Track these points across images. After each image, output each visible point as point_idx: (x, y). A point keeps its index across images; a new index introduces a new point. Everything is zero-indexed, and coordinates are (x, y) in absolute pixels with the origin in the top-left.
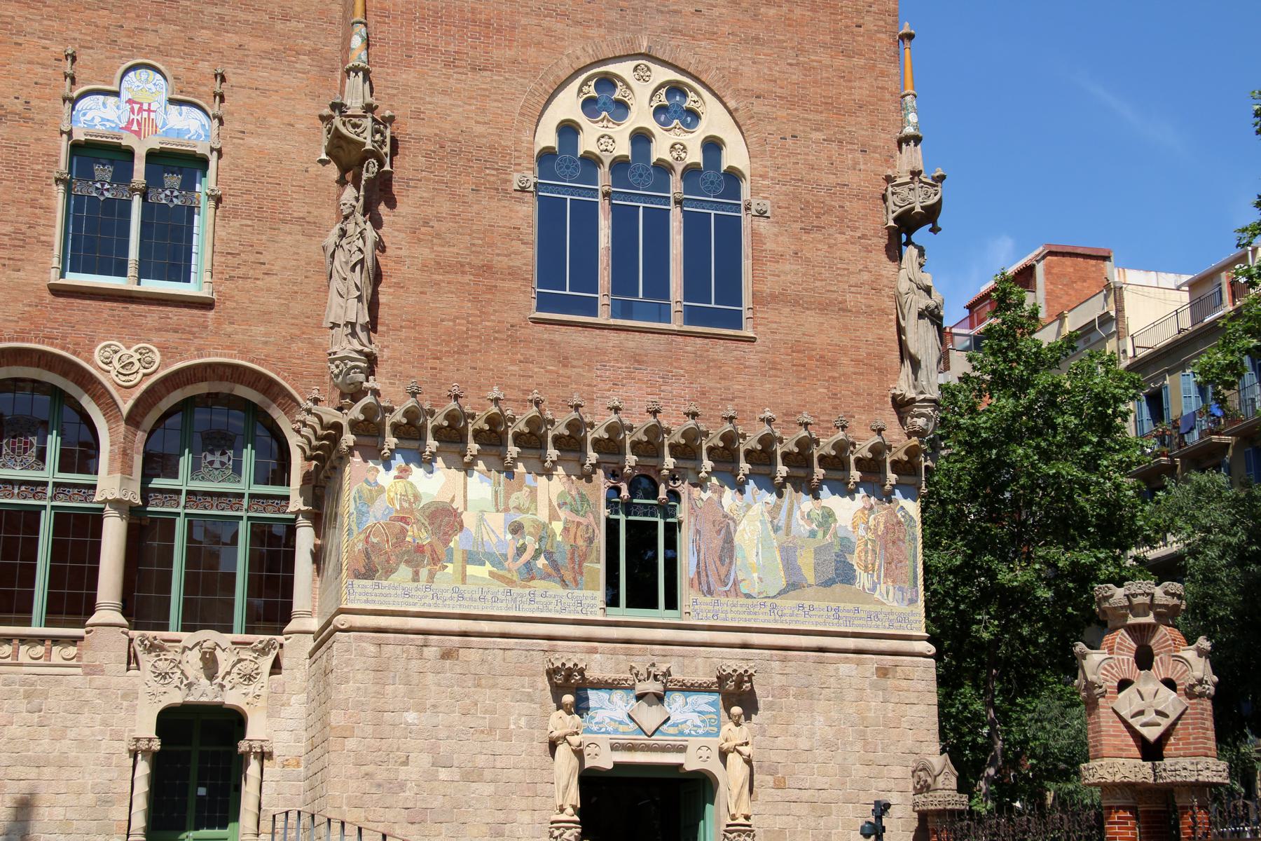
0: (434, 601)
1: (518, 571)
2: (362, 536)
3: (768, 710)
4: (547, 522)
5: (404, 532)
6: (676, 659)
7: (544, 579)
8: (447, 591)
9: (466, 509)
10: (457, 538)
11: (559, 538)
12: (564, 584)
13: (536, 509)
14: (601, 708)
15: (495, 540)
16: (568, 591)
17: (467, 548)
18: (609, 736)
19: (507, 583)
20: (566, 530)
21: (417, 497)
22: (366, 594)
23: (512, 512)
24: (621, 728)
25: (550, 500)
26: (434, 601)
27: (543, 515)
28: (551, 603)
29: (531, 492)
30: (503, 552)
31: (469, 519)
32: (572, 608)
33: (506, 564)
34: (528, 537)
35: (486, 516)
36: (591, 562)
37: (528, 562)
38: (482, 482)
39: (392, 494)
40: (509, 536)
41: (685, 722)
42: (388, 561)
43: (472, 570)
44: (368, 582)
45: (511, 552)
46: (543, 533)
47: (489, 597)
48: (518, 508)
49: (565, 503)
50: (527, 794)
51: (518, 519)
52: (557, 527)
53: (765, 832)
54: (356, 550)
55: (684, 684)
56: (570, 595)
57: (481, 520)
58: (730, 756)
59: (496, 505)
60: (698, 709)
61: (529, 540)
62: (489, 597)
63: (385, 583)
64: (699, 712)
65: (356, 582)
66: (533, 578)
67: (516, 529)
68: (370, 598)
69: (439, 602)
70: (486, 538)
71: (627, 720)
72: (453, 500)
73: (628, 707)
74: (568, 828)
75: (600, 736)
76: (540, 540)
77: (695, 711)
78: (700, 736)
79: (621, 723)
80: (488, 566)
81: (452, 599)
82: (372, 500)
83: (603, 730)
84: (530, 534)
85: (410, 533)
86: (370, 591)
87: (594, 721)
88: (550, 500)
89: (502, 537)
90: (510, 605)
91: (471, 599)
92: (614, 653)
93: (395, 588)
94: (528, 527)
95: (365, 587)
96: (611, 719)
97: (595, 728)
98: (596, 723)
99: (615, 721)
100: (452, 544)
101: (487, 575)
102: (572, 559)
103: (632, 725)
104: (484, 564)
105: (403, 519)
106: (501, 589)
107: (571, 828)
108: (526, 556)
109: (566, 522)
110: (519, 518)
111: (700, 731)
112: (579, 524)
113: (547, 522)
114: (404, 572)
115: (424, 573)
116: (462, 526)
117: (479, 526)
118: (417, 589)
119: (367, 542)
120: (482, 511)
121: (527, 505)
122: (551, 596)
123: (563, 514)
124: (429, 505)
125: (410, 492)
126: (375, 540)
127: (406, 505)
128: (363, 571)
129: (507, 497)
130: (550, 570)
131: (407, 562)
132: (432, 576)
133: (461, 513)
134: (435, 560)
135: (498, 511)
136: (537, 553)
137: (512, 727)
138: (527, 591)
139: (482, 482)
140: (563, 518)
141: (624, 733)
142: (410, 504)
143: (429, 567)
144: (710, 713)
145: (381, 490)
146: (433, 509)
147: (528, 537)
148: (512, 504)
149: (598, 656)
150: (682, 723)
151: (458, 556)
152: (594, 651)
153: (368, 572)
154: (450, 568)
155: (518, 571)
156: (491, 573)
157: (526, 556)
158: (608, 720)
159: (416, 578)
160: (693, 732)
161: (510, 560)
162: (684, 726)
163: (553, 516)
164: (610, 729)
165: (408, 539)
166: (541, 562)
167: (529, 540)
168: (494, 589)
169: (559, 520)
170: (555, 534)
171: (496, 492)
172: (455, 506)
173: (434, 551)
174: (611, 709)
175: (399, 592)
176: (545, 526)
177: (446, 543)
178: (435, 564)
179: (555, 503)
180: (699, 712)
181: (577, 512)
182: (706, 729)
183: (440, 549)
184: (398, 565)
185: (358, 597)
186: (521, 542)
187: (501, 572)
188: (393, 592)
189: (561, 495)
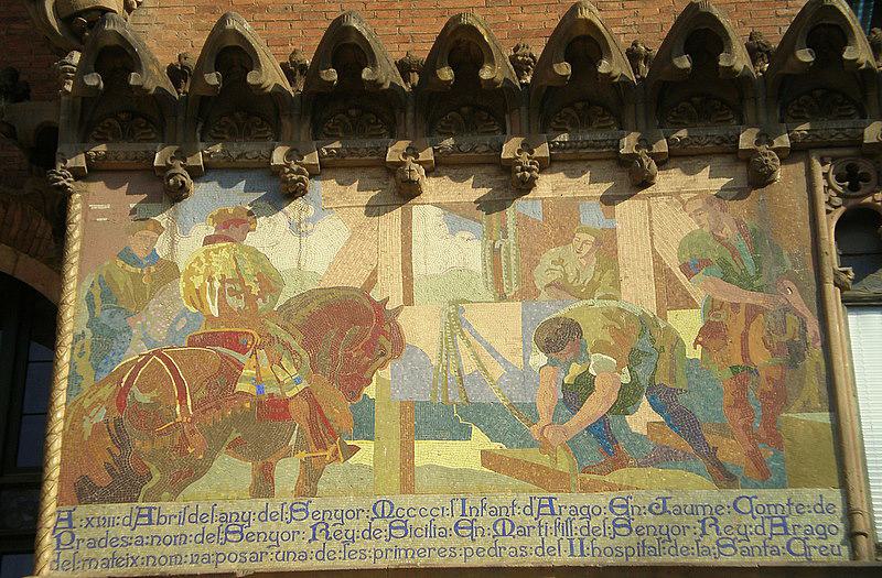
0: (317, 545)
1: (572, 446)
2: (107, 391)
4: (651, 308)
5: (231, 372)
7: (656, 462)
8: (356, 514)
9: (409, 300)
10: (385, 374)
11: (693, 353)
12: (724, 476)
13: (616, 283)
15: (497, 371)
16: (738, 492)
17: (416, 397)
19: (540, 483)
20: (711, 333)
21: (269, 282)
22: (113, 542)
23: (544, 296)
25: (657, 259)
26: (317, 545)
27: (639, 294)
28: (683, 529)
29: (598, 242)
30: (519, 399)
31: (421, 327)
32: (755, 541)
33: (534, 430)
34: (595, 358)
35: (470, 313)
36: (806, 408)
37: (603, 420)
38: (453, 232)
39: (198, 281)
40: (539, 359)
42: (181, 448)
43: (431, 453)
44: (120, 510)
45: (546, 398)
46: (637, 342)
47: (485, 521)
48: (558, 286)
49: (707, 263)
51: (562, 313)
52: (686, 324)
54: (87, 426)
56: (744, 506)
57: (456, 322)
59: (498, 283)
61: (598, 363)
62: (485, 521)
63: (170, 508)
65: (82, 511)
66: (619, 463)
67: (559, 338)
68: (121, 552)
69: (335, 545)
70: (469, 366)
72: (371, 282)
76: (634, 359)
80: (479, 439)
81: (371, 534)
82: (141, 299)
84: (601, 347)
85: (246, 372)
86: (124, 531)
88: (657, 259)
89: (518, 361)
90: (551, 542)
91: (430, 531)
93: (202, 519)
94: (594, 331)
95: (107, 522)
100: (370, 391)
101: (476, 465)
102: (741, 402)
104: (465, 434)
105: (234, 341)
106: (523, 500)
108: (594, 407)
109: (712, 307)
110: (569, 309)
112: (753, 312)
113: (651, 308)
114: (230, 474)
115: (287, 472)
116: (399, 344)
117: (448, 345)
118: (265, 515)
119: (121, 406)
120: (455, 303)
121: (588, 275)
122: (679, 510)
123: (698, 289)
124: (304, 299)
125: (248, 270)
126: (145, 398)
127: (235, 303)
128: (103, 479)
129: (530, 260)
130: (672, 439)
131: (235, 445)
132: (310, 479)
133: (397, 311)
134: (323, 432)
135: (502, 298)
136: (625, 401)
138: (603, 499)
139: (453, 232)
140: (699, 296)
142: (251, 300)
143: (303, 455)
145: (168, 271)
146: (314, 307)
147: (595, 358)
148: (542, 277)
151: (387, 421)
153: (125, 485)
154: (366, 452)
155: (572, 446)
156: (486, 457)
157: (594, 407)
159: (264, 484)
161: (545, 419)
163: (674, 298)
165: (241, 387)
166: (642, 418)
167: (598, 363)
168: (505, 499)
169: (690, 304)
170: (678, 342)
171: (495, 252)
172: (376, 295)
173: (316, 408)
175: (211, 528)
176: (644, 324)
177: (354, 382)
178: (322, 446)
179: (673, 262)
181: (745, 283)
183: (338, 409)
184: (211, 457)
185: (84, 553)
186: (575, 369)
187: (517, 453)
188: (196, 529)
189: (688, 243)
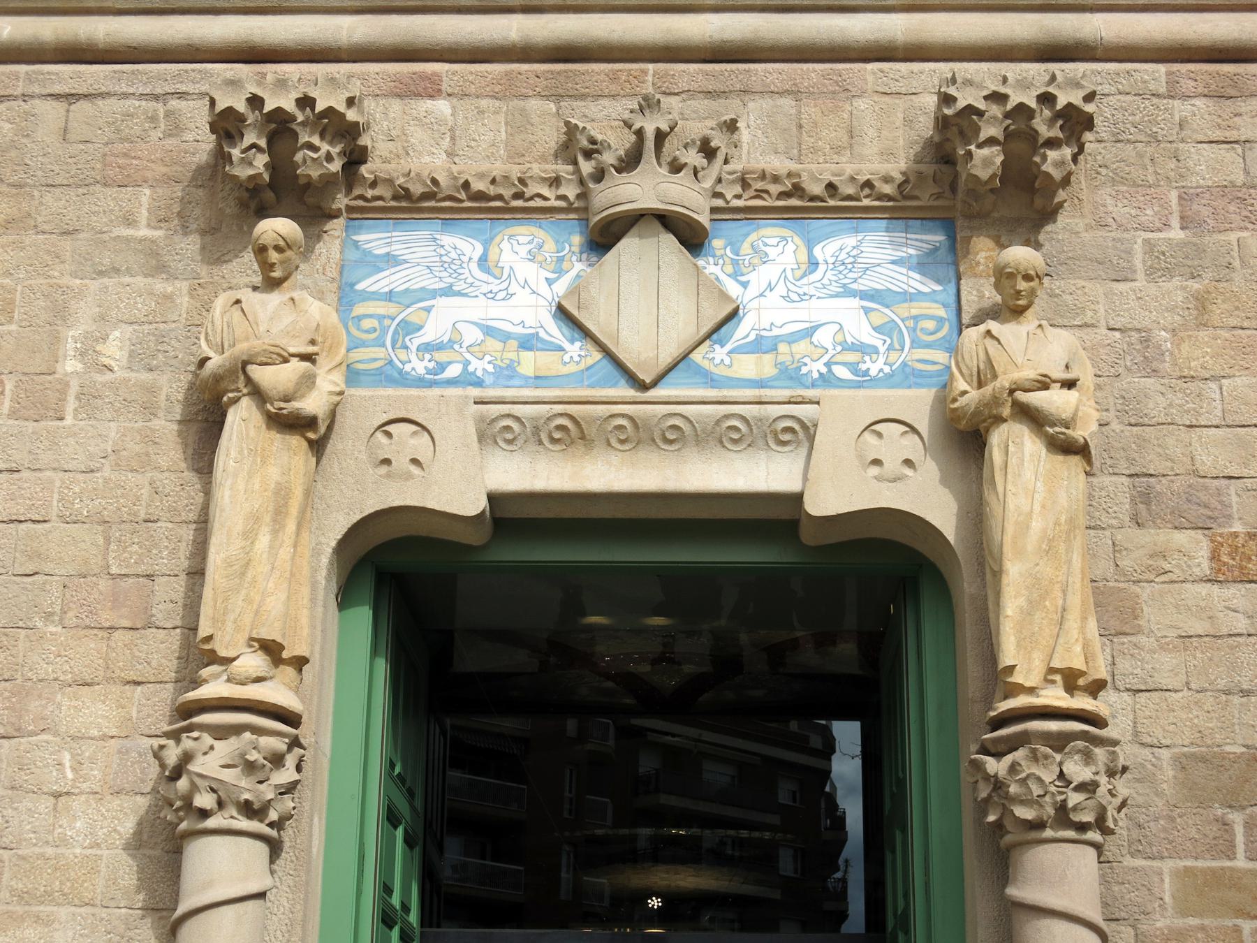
3: (1169, 273)
6: (766, 103)
14: (448, 292)
18: (475, 392)
24: (529, 363)
41: (810, 332)
50: (107, 618)
53: (1182, 763)
55: (797, 190)
58: (996, 439)
60: (866, 284)
64: (864, 295)
71: (555, 331)
73: (561, 287)
74: (222, 732)
75: (436, 391)
77: (847, 292)
78: (874, 382)
79: (527, 343)
83: (453, 371)
87: (415, 342)
92: (506, 91)
96: (489, 331)
97: (419, 366)
98: (426, 348)
99: (505, 337)
103: (576, 349)
107: (237, 730)
111: (875, 367)
137: (71, 365)
141: (539, 380)
144: (908, 297)
149: (442, 107)
150: (792, 338)
152: (432, 90)
158: (472, 335)
160: (841, 372)
162: (801, 347)
164: (479, 366)
174: (491, 296)
180: (864, 295)
182: (898, 359)
